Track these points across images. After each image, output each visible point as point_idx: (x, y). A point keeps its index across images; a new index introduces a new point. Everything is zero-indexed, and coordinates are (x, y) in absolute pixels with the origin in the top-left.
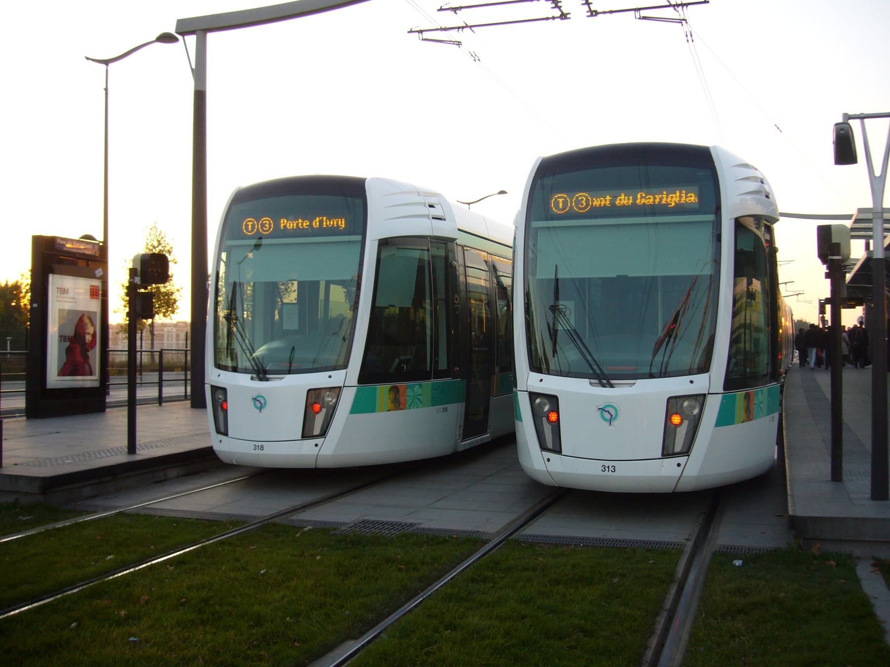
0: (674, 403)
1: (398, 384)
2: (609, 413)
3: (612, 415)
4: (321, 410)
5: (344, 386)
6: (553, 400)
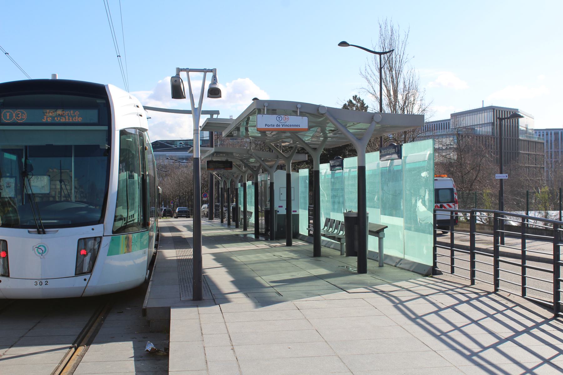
0: (83, 242)
3: (43, 251)
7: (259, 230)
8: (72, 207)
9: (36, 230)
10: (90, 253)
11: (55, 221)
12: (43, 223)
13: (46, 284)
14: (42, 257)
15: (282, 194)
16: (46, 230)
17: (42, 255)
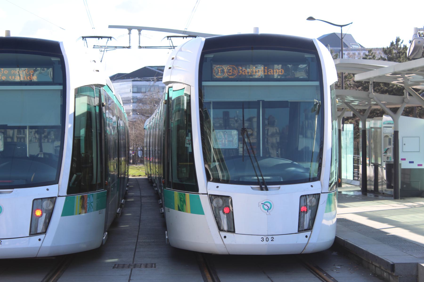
0: (304, 197)
1: (85, 194)
2: (267, 206)
3: (269, 207)
6: (226, 199)
9: (259, 186)
12: (266, 179)
13: (272, 241)
14: (268, 213)
15: (405, 144)
16: (268, 186)
17: (268, 212)
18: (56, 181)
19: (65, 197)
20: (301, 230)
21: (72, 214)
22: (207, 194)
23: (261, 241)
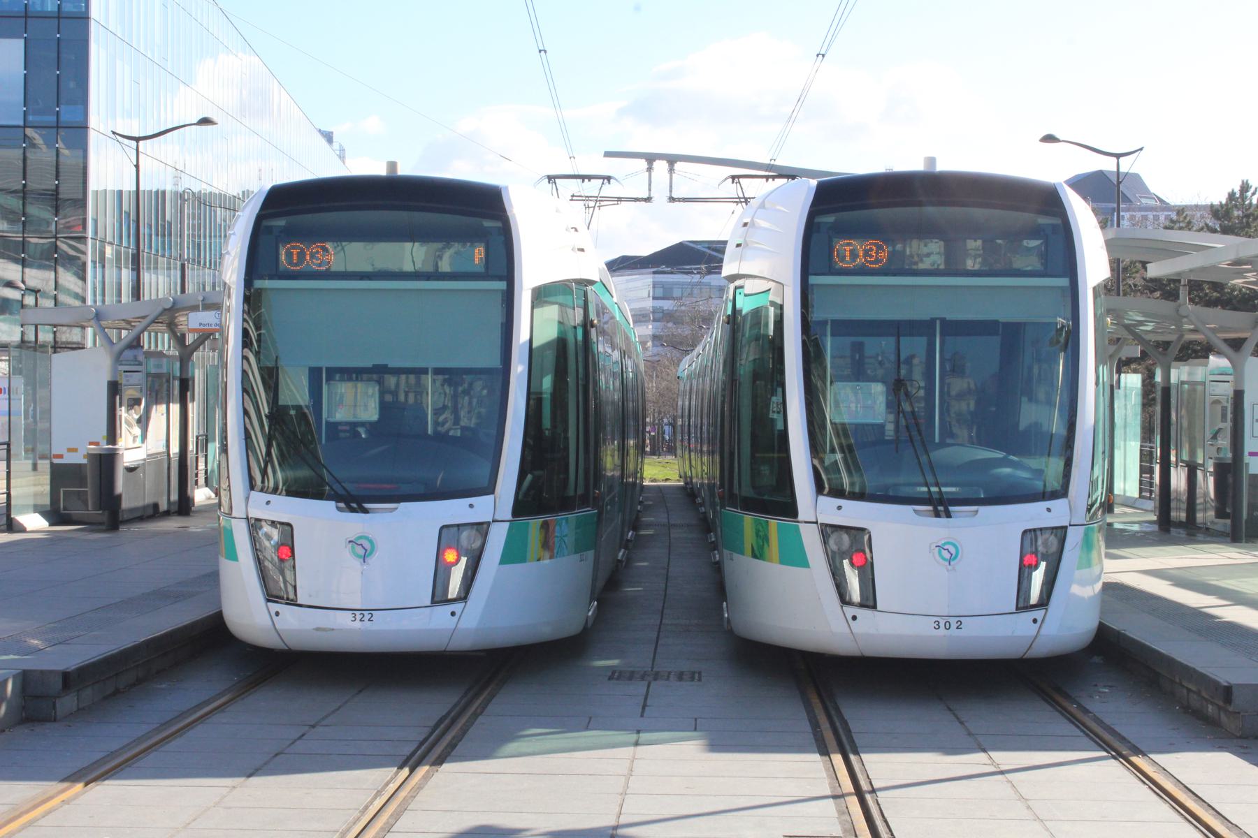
0: (1030, 535)
1: (549, 518)
4: (458, 561)
5: (493, 521)
6: (857, 534)
7: (1172, 514)
8: (979, 457)
9: (930, 508)
10: (1045, 563)
11: (953, 489)
12: (947, 493)
13: (957, 628)
14: (950, 568)
16: (951, 509)
17: (950, 564)
18: (489, 489)
19: (508, 523)
20: (1023, 606)
21: (522, 559)
22: (816, 523)
23: (935, 628)
